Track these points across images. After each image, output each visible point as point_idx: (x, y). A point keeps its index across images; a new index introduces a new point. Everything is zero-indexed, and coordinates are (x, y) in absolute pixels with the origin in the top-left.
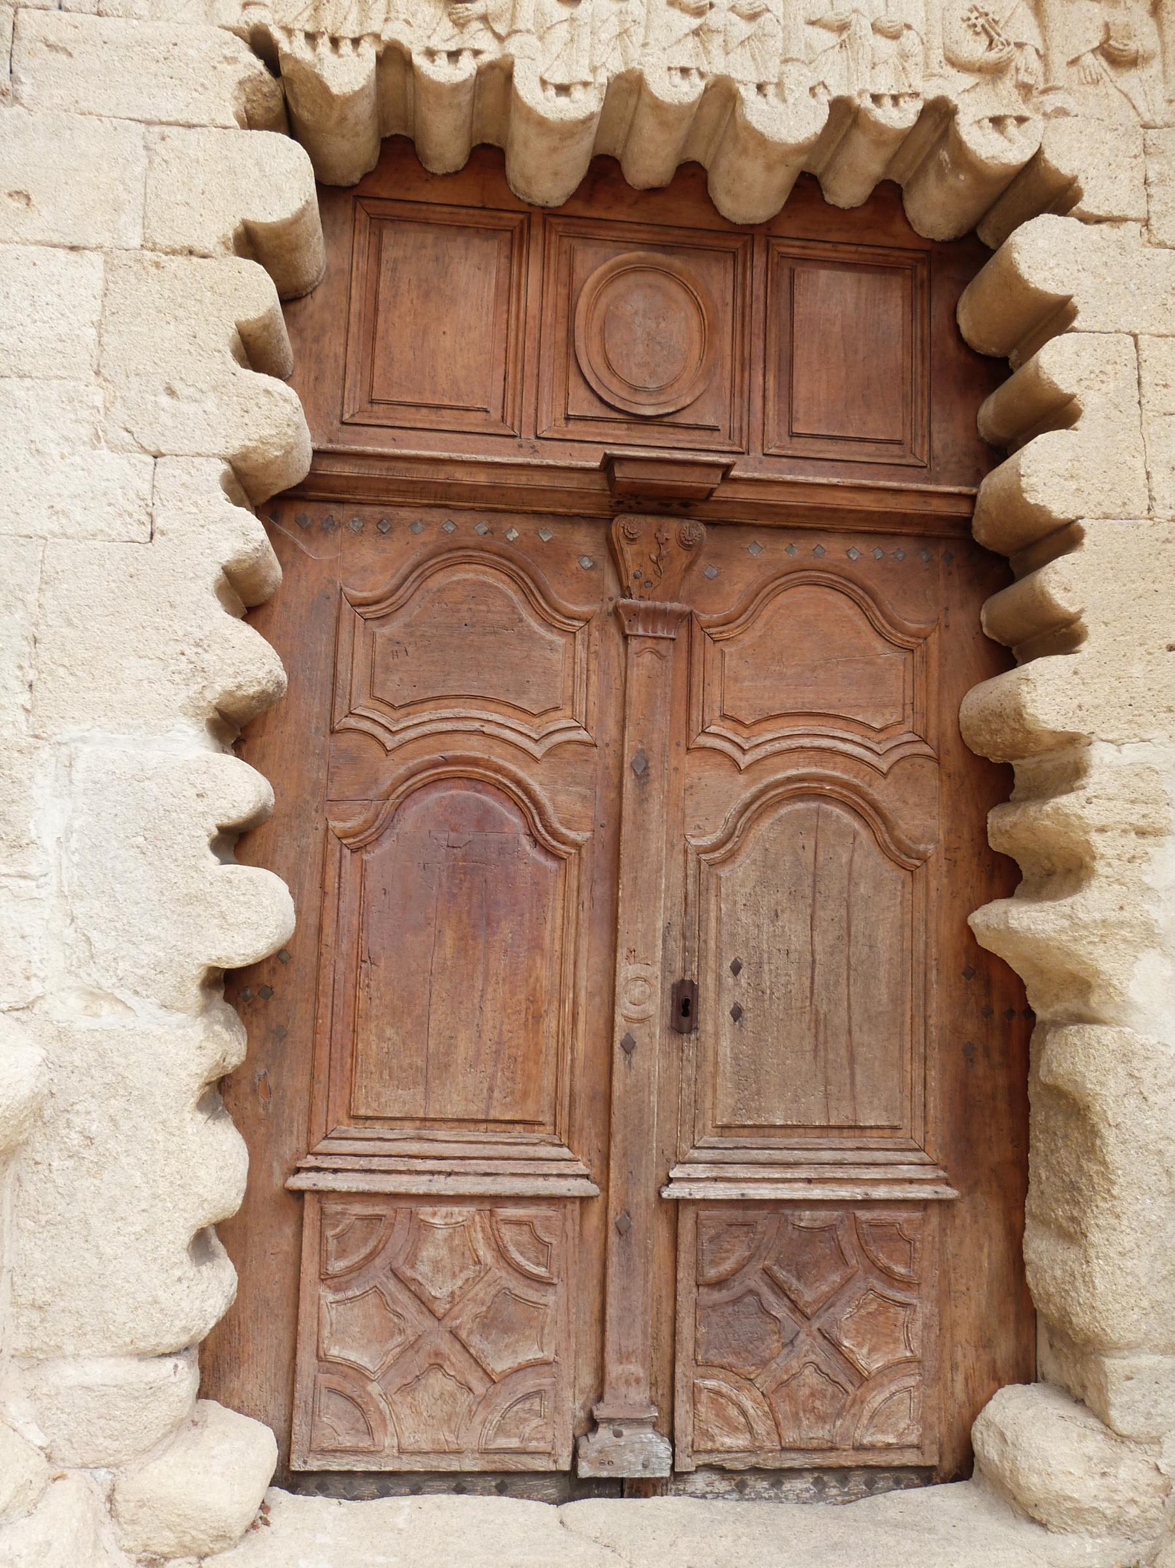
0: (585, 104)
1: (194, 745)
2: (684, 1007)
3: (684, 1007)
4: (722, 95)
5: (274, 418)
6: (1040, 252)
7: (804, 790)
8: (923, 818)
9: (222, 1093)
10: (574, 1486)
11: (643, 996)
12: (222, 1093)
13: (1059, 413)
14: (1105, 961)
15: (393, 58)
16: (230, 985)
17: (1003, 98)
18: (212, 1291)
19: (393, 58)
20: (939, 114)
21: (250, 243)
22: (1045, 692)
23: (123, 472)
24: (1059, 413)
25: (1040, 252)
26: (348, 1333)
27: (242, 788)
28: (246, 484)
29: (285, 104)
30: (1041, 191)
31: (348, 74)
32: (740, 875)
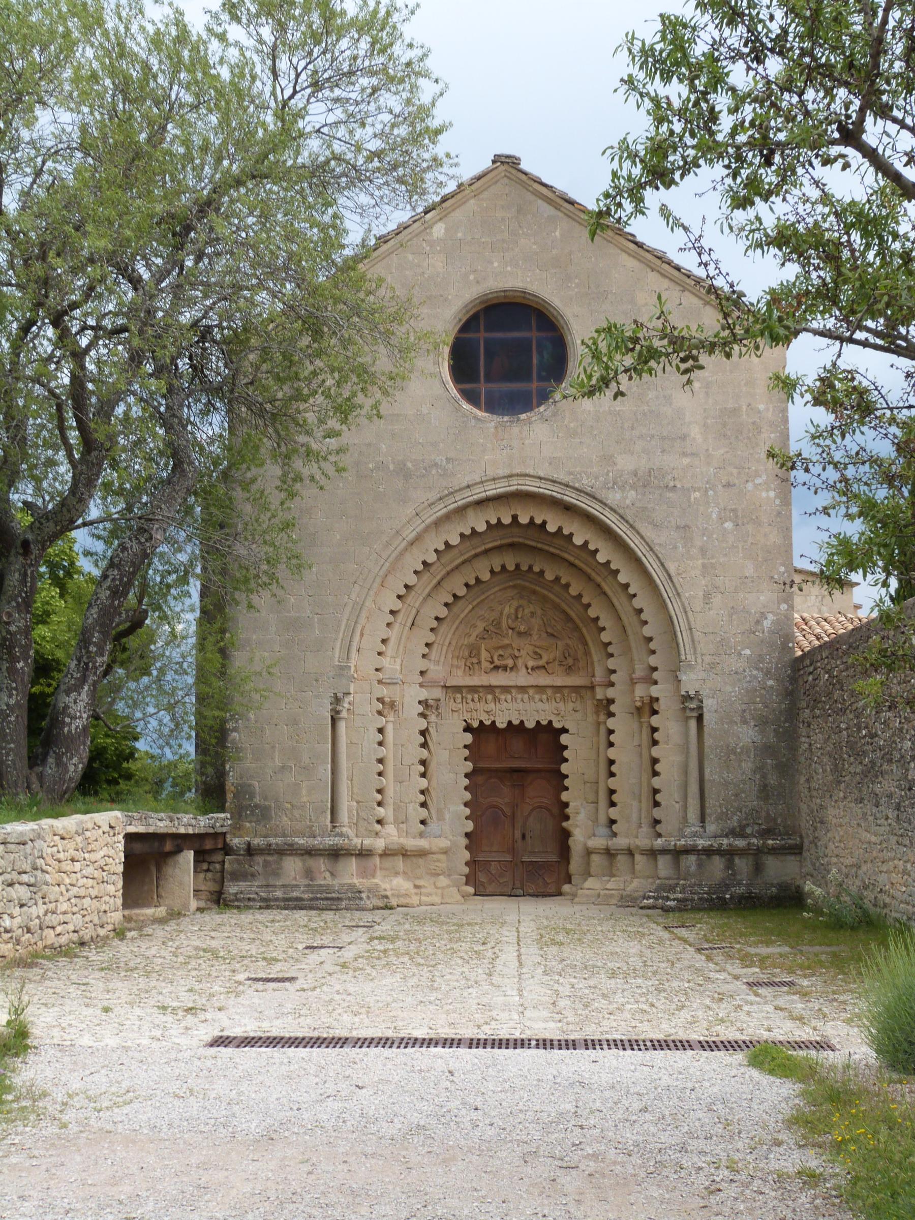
0: (505, 725)
1: (462, 807)
2: (524, 836)
3: (524, 836)
4: (522, 722)
5: (469, 766)
6: (564, 739)
7: (540, 807)
8: (556, 811)
9: (467, 848)
10: (510, 896)
11: (518, 834)
12: (467, 848)
13: (566, 760)
14: (571, 829)
15: (481, 722)
16: (467, 835)
17: (559, 718)
18: (466, 870)
19: (481, 722)
20: (550, 722)
21: (465, 747)
22: (565, 796)
23: (452, 776)
24: (566, 760)
25: (564, 739)
26: (482, 877)
27: (468, 811)
28: (467, 776)
29: (468, 729)
30: (565, 730)
31: (475, 724)
32: (531, 819)
